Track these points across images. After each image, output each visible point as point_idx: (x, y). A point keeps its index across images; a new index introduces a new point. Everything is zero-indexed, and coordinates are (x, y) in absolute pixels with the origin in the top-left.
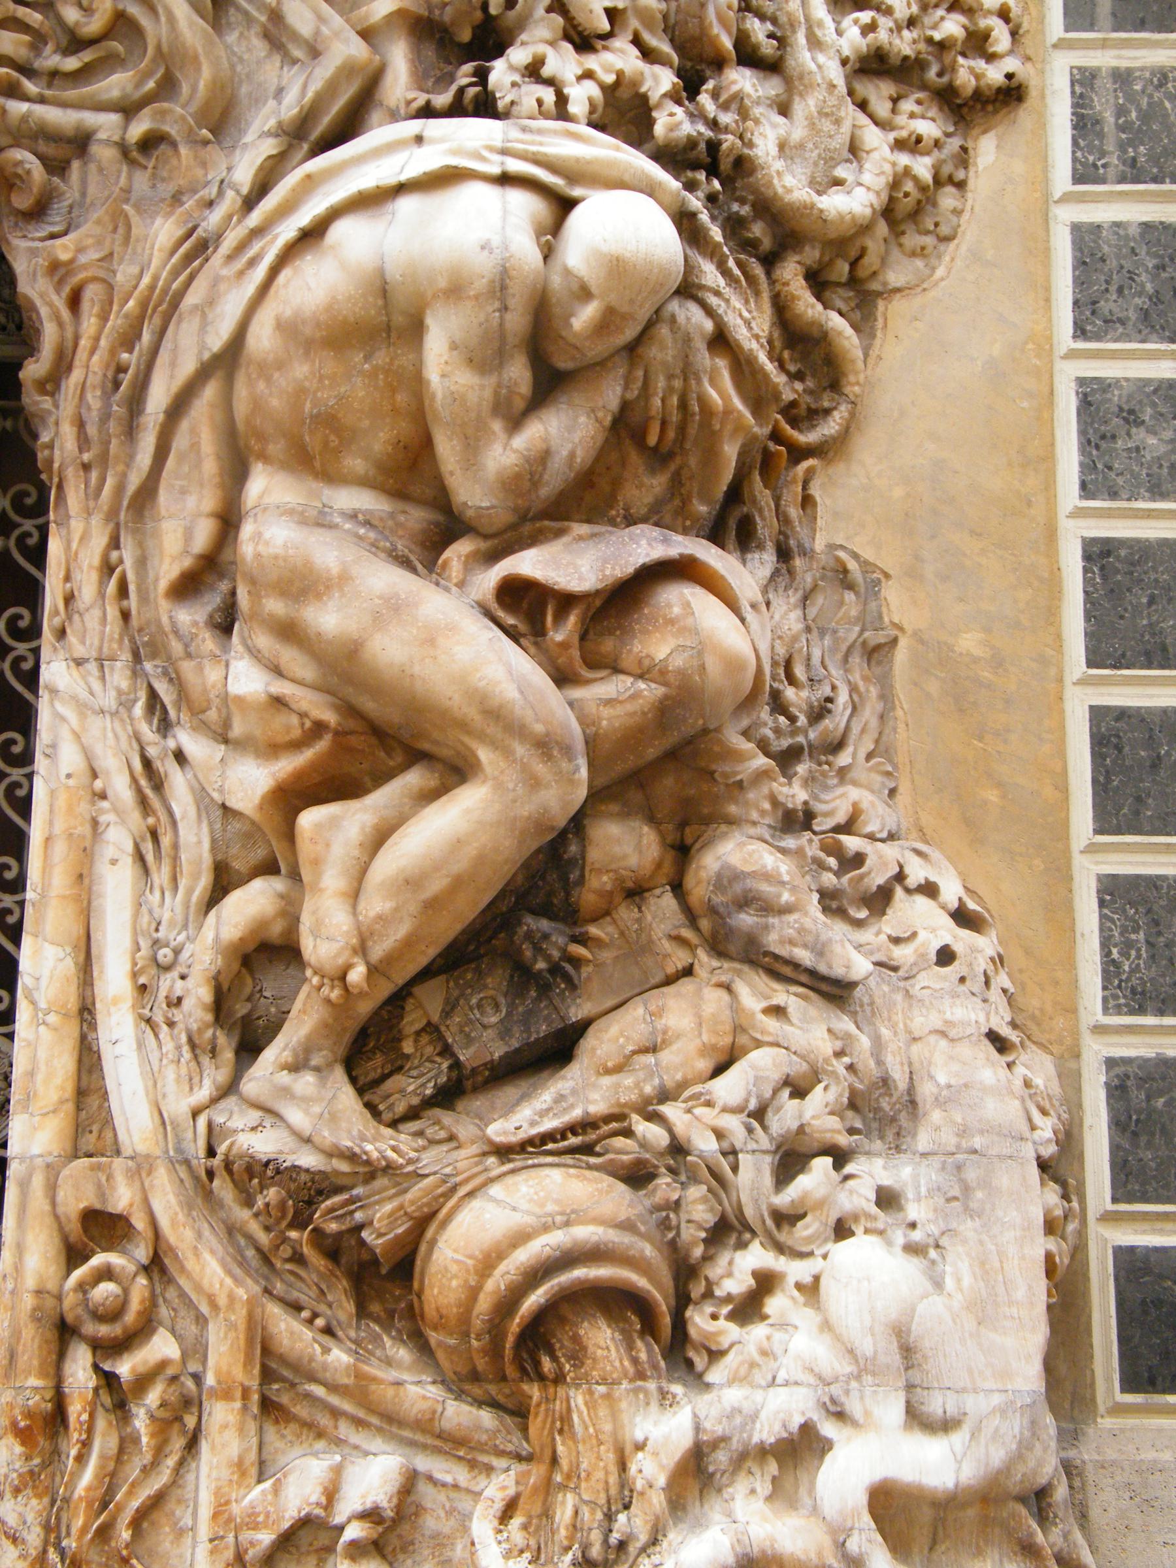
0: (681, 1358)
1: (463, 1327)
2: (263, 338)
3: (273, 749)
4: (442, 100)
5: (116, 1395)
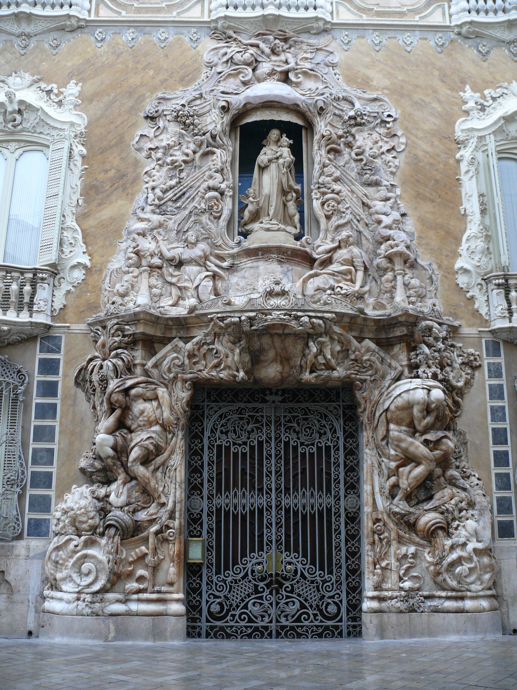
0: (449, 535)
1: (424, 531)
2: (392, 407)
3: (395, 461)
4: (413, 375)
5: (381, 540)
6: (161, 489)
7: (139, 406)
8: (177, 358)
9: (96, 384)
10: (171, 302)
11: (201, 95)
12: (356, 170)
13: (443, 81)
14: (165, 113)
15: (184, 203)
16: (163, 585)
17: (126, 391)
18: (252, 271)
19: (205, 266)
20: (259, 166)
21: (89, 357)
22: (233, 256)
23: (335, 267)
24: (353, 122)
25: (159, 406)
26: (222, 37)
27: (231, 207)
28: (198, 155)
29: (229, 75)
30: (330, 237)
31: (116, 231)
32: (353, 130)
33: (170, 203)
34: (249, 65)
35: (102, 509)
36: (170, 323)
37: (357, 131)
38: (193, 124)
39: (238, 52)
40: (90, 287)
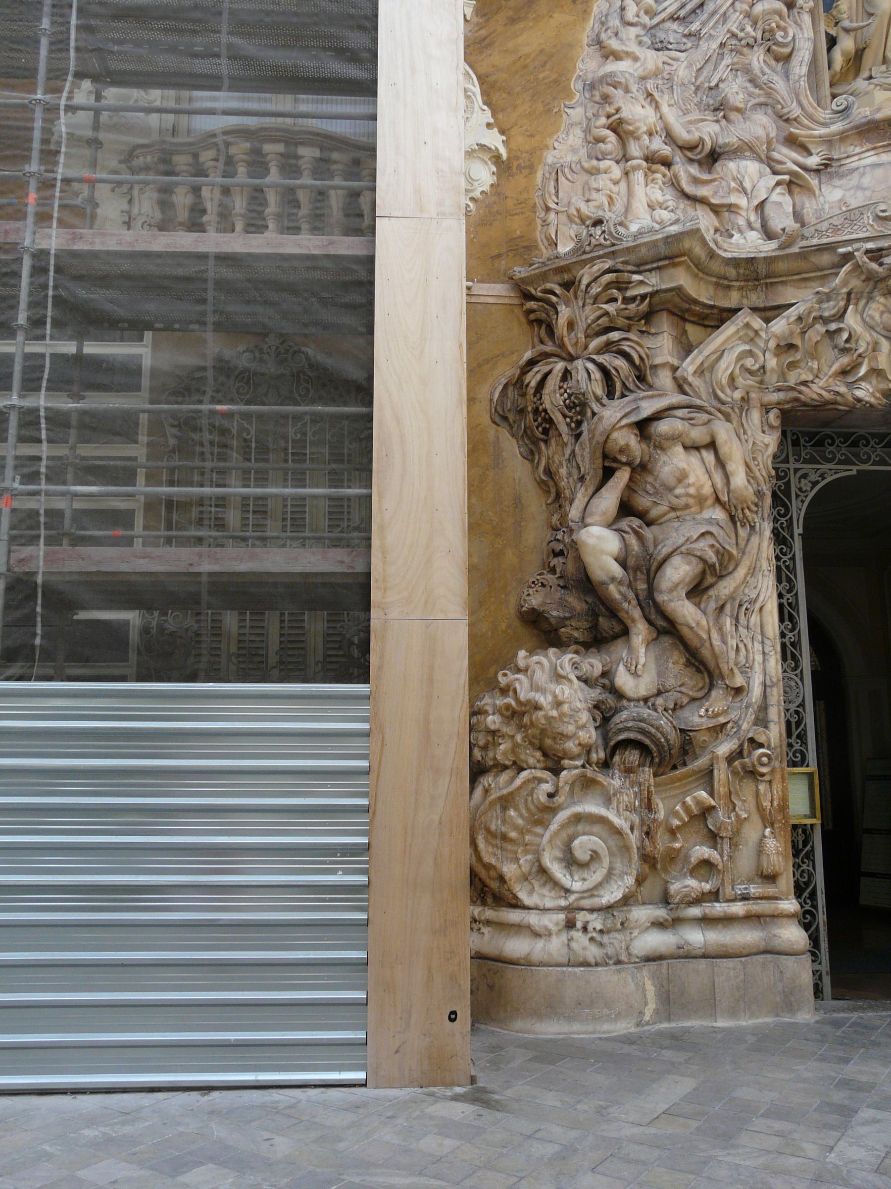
6: (732, 655)
7: (676, 461)
8: (750, 353)
9: (558, 417)
15: (704, 24)
16: (750, 881)
17: (643, 427)
18: (879, 172)
21: (528, 355)
22: (828, 141)
25: (721, 463)
31: (556, 81)
33: (675, 26)
35: (596, 707)
36: (732, 272)
40: (510, 203)
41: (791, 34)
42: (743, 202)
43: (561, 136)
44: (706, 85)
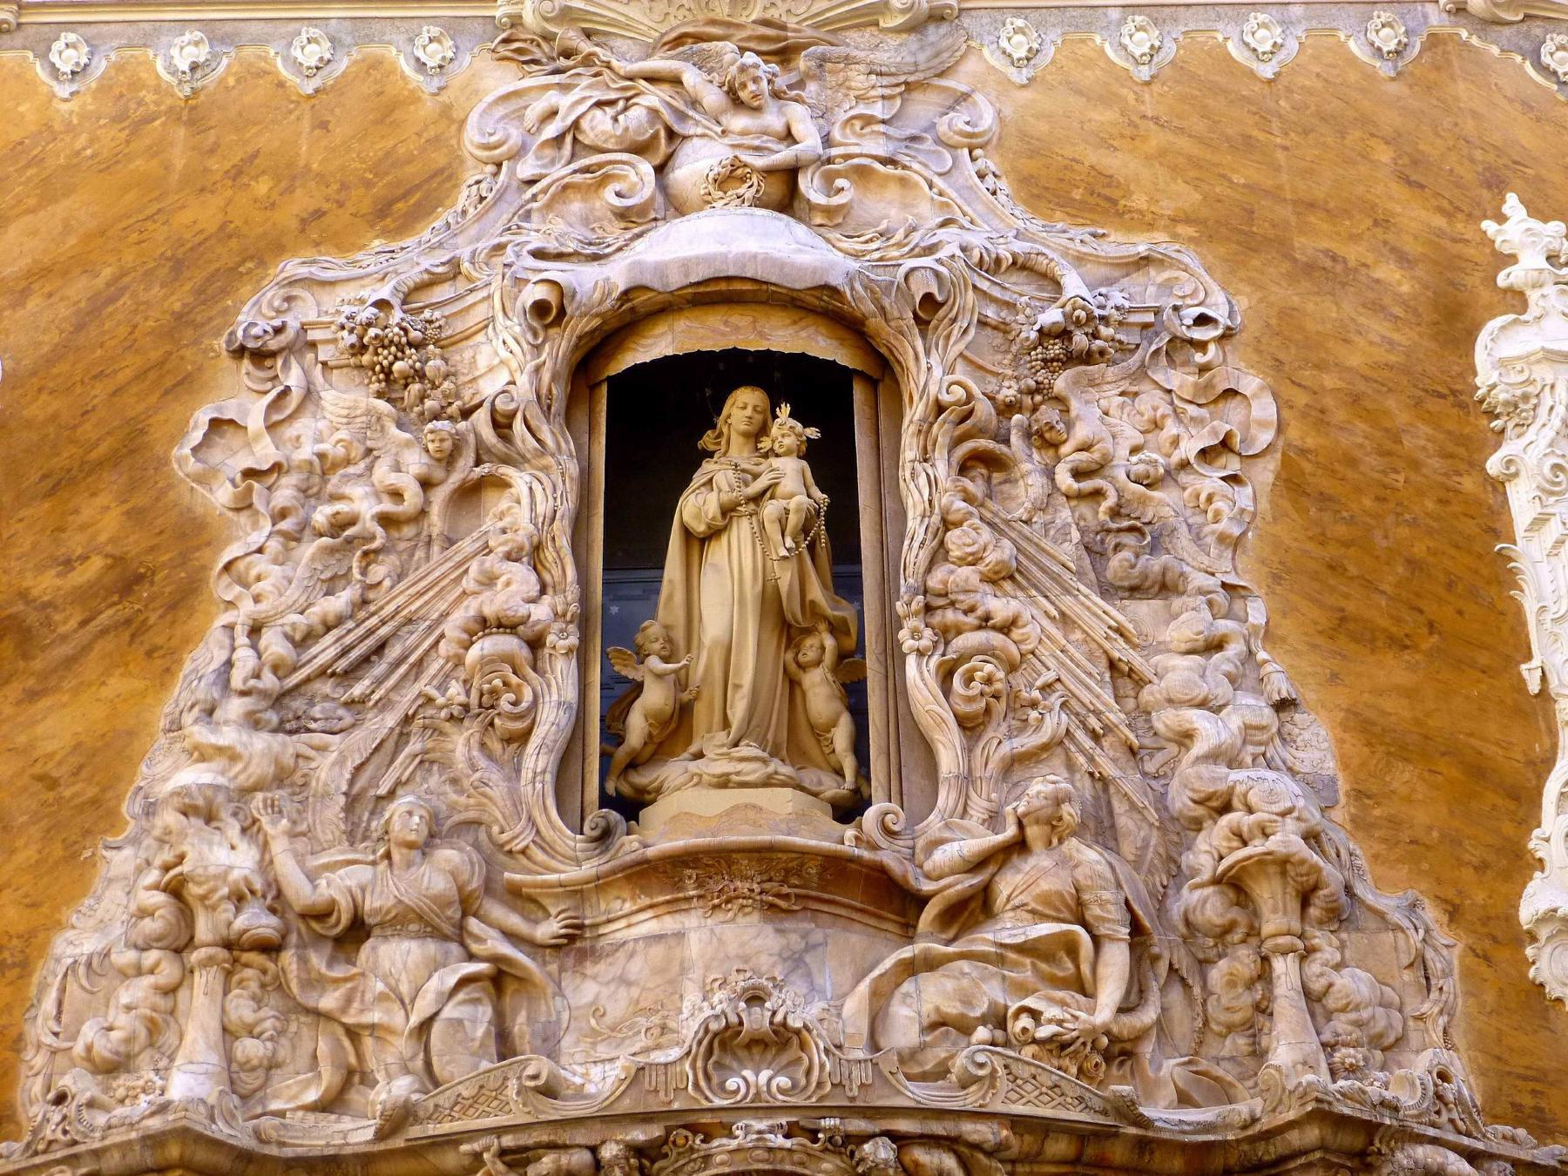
10: (312, 1096)
11: (454, 264)
12: (1076, 535)
13: (1409, 182)
14: (313, 335)
15: (379, 682)
18: (657, 951)
19: (460, 935)
20: (687, 533)
22: (577, 893)
23: (1010, 929)
24: (1056, 349)
26: (538, 55)
27: (571, 695)
28: (440, 496)
29: (565, 187)
30: (979, 806)
31: (95, 802)
32: (1061, 383)
33: (326, 687)
34: (641, 149)
37: (1076, 382)
38: (420, 375)
39: (600, 104)
41: (528, 696)
42: (397, 1019)
43: (88, 901)
44: (372, 793)
